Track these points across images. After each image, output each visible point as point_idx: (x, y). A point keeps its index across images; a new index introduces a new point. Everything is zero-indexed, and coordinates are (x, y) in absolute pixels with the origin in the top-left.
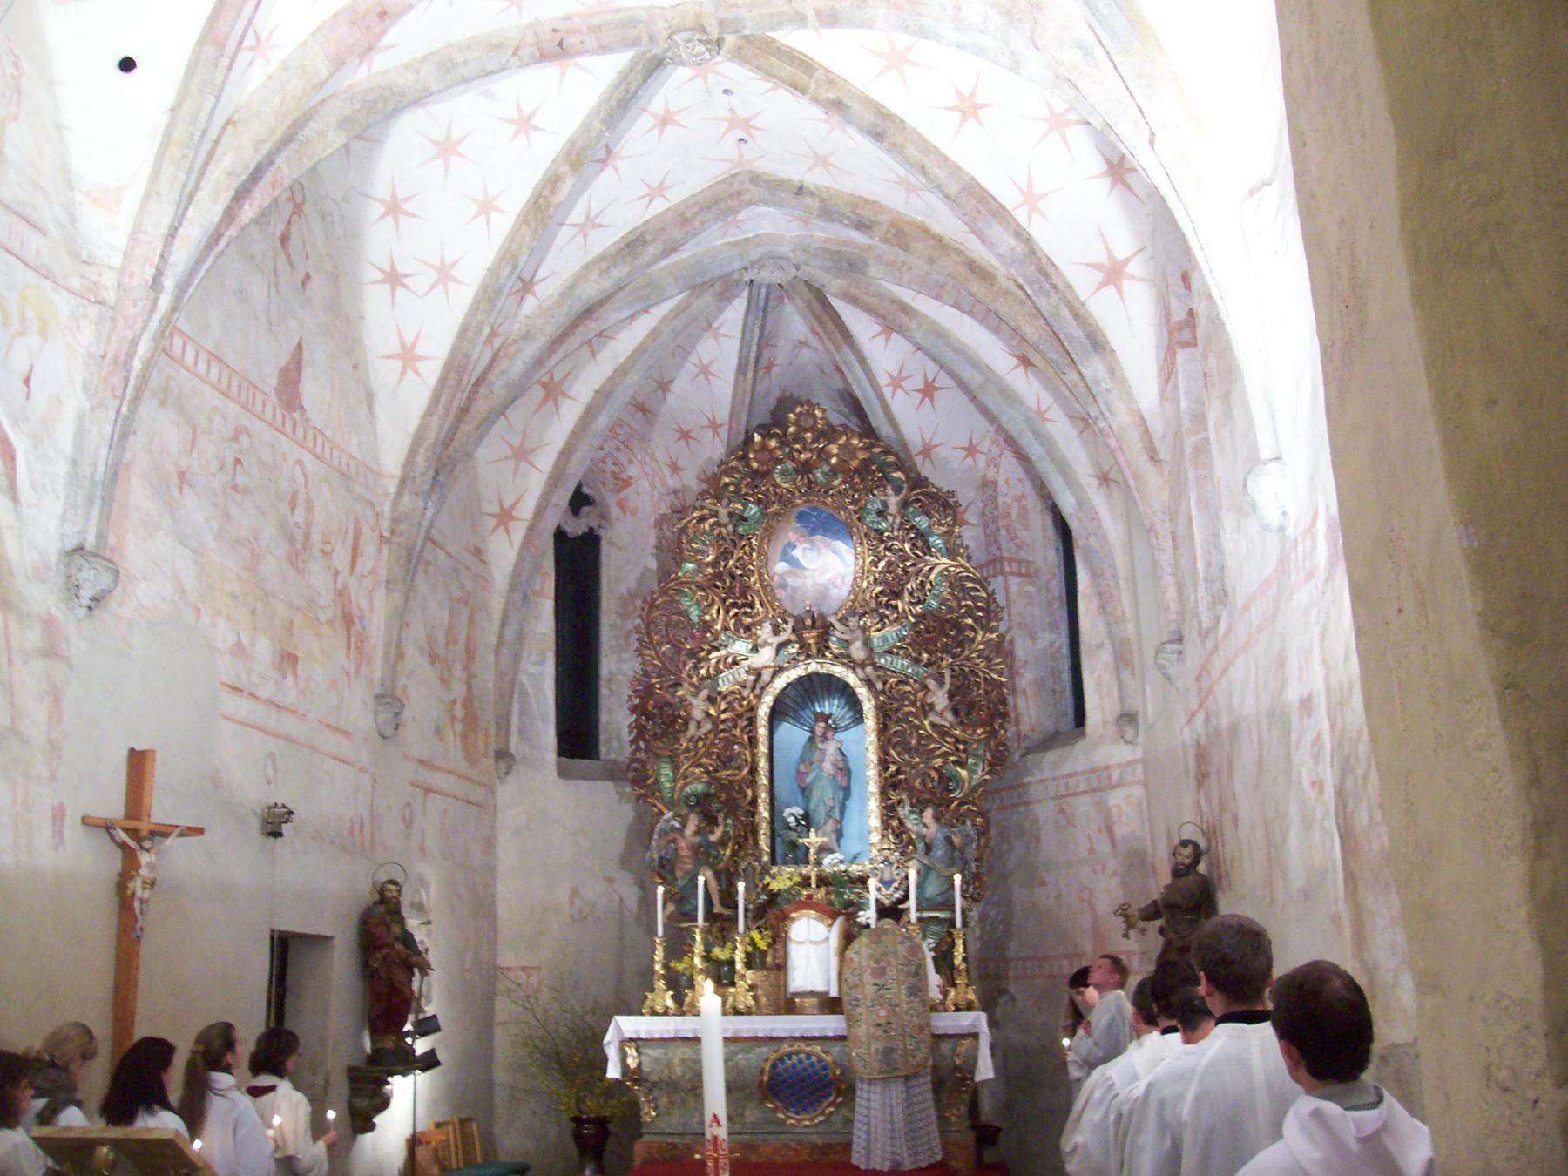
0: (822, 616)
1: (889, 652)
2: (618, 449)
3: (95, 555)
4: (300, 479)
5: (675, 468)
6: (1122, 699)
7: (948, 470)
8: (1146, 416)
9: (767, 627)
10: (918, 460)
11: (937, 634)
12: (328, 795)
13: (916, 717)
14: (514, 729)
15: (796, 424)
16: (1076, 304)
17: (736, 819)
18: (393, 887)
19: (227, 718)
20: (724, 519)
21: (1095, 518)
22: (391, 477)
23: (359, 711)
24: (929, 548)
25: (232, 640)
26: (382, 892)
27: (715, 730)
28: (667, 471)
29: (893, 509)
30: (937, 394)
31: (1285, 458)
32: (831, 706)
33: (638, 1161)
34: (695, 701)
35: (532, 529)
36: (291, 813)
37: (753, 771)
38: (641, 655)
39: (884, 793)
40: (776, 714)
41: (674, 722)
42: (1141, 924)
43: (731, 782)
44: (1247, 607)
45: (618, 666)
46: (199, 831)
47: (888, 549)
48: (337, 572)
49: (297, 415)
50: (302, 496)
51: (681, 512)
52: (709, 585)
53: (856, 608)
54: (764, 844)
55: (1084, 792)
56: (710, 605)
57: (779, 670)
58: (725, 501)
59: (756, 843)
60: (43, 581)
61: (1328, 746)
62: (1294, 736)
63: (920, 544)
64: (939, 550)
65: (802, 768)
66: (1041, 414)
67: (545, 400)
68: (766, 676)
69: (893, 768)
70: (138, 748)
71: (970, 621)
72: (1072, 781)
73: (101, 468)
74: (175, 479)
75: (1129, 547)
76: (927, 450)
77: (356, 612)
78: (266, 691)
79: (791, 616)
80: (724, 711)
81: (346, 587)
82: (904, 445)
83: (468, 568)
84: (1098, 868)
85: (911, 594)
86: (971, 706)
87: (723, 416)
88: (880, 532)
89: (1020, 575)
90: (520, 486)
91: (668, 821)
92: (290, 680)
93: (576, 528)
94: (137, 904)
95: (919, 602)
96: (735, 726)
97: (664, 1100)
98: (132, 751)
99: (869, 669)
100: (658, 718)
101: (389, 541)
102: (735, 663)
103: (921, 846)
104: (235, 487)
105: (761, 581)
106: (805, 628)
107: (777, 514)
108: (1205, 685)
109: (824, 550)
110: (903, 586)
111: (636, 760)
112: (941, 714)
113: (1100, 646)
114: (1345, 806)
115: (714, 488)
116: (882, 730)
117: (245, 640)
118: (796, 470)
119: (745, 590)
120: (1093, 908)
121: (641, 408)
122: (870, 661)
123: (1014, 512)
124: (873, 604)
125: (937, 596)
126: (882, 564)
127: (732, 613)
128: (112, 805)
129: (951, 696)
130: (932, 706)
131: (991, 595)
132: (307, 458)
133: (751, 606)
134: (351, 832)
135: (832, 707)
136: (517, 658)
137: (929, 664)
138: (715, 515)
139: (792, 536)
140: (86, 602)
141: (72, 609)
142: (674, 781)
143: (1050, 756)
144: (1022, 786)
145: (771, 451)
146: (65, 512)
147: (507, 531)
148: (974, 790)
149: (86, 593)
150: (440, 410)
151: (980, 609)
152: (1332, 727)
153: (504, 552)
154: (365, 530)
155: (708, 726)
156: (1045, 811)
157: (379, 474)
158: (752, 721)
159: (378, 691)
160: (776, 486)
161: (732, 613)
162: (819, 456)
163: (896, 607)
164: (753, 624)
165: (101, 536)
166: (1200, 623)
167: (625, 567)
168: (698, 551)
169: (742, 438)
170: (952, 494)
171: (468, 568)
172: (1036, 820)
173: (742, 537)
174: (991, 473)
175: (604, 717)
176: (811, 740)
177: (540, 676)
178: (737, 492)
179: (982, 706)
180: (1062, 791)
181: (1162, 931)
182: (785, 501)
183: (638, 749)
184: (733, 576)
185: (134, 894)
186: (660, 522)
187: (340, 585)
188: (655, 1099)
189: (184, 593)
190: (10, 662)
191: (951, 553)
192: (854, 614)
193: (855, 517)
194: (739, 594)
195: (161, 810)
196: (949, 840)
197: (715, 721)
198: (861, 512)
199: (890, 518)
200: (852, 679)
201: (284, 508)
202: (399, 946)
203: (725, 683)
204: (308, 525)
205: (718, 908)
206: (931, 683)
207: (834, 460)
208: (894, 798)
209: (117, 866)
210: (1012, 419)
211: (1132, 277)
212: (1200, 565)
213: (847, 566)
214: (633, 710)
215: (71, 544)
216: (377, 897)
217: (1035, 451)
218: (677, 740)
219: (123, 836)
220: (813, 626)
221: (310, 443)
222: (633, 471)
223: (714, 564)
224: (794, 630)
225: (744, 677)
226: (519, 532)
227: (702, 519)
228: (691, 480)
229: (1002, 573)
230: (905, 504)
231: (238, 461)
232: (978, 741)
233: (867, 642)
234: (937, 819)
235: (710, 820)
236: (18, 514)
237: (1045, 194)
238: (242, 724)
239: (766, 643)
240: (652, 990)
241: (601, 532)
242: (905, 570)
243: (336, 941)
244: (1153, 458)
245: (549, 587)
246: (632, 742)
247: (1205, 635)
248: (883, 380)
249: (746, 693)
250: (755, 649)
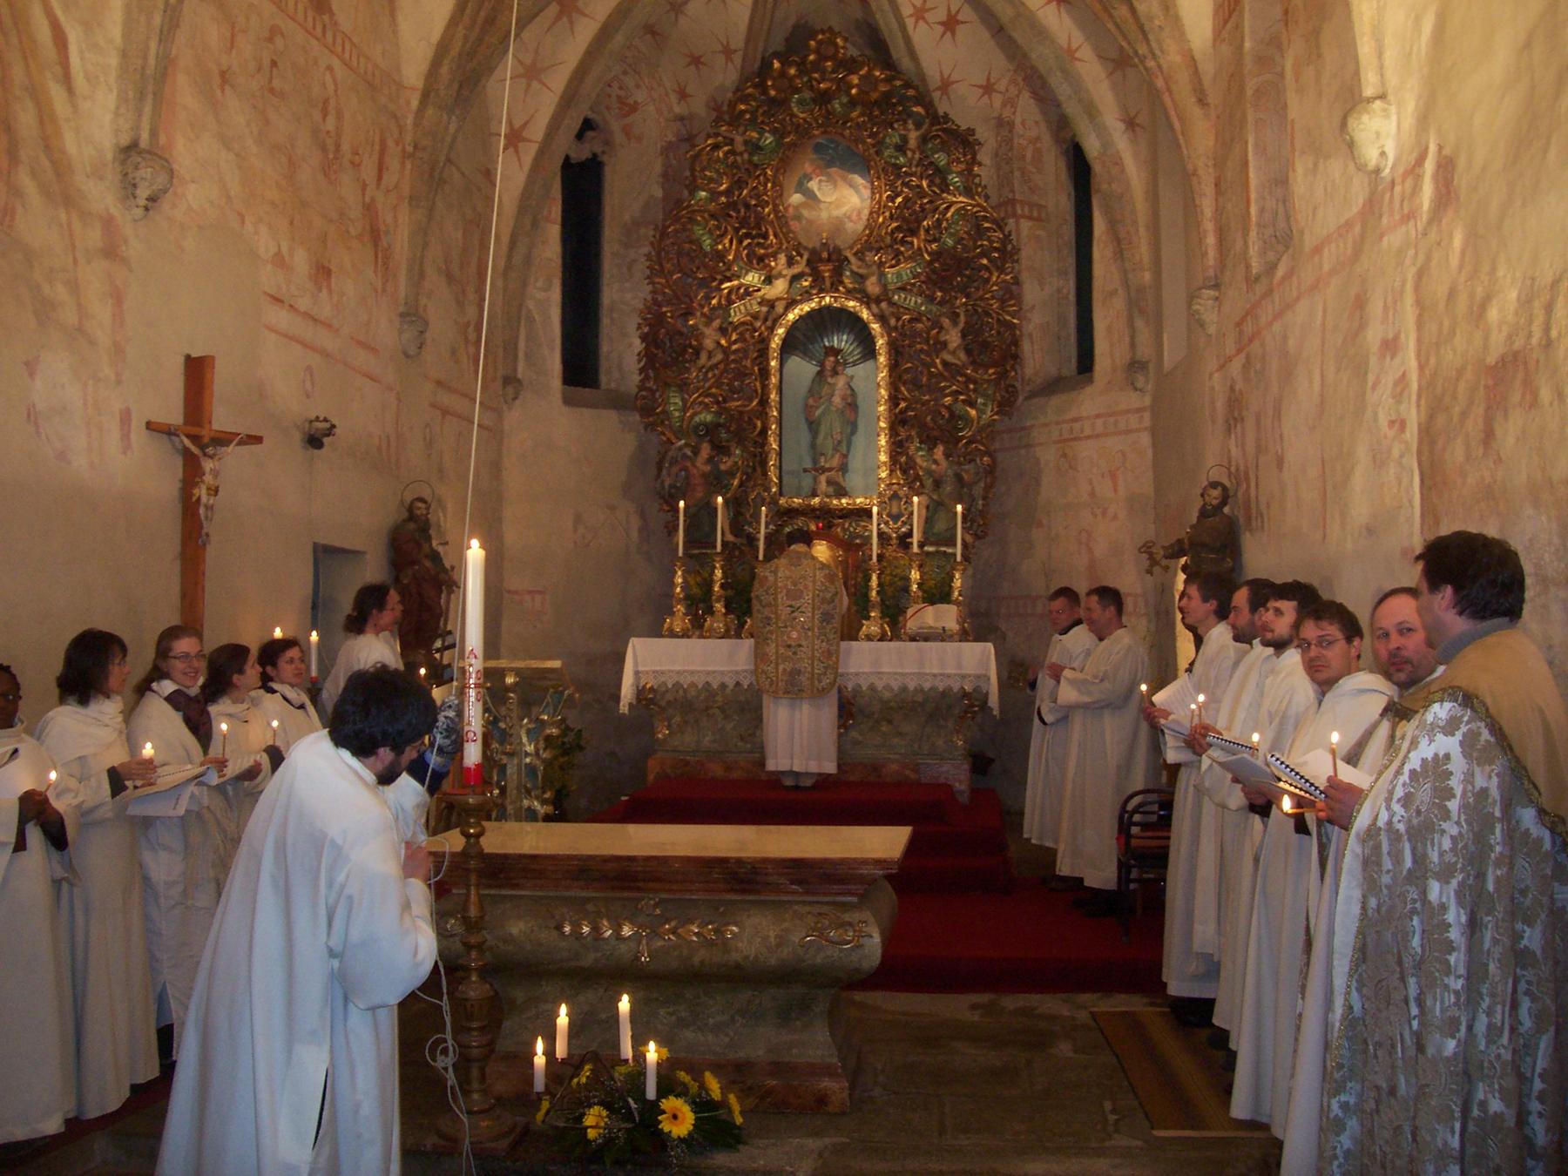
0: (838, 250)
1: (903, 289)
2: (625, 73)
3: (149, 152)
4: (331, 87)
5: (683, 95)
6: (1133, 345)
7: (966, 107)
8: (1197, 55)
9: (782, 258)
10: (936, 95)
11: (950, 273)
12: (360, 414)
13: (928, 354)
14: (521, 355)
15: (817, 52)
17: (744, 449)
18: (420, 504)
19: (267, 327)
20: (740, 147)
21: (1118, 162)
22: (413, 89)
23: (386, 330)
24: (947, 186)
25: (274, 250)
26: (410, 509)
27: (726, 360)
28: (673, 98)
29: (912, 143)
30: (960, 29)
31: (1391, 97)
32: (840, 341)
33: (651, 778)
34: (708, 331)
35: (541, 152)
36: (333, 426)
37: (764, 402)
38: (653, 283)
39: (893, 431)
40: (788, 347)
41: (684, 351)
42: (1164, 562)
43: (741, 413)
44: (1318, 250)
45: (624, 296)
46: (258, 440)
47: (905, 184)
48: (364, 187)
49: (326, 18)
50: (332, 102)
51: (690, 139)
52: (721, 215)
53: (871, 242)
54: (773, 475)
55: (1088, 437)
56: (723, 236)
57: (791, 304)
58: (741, 129)
59: (765, 474)
60: (101, 178)
61: (1415, 386)
62: (1371, 378)
63: (937, 181)
64: (957, 188)
65: (811, 401)
66: (1071, 53)
67: (558, 18)
68: (780, 308)
69: (903, 405)
70: (194, 355)
71: (985, 261)
72: (1077, 426)
73: (152, 62)
74: (217, 81)
75: (1153, 196)
76: (945, 86)
77: (382, 228)
78: (304, 303)
79: (806, 248)
80: (735, 342)
81: (373, 199)
82: (923, 79)
83: (479, 190)
84: (1099, 511)
85: (927, 231)
86: (985, 345)
87: (738, 42)
88: (898, 167)
89: (1030, 218)
90: (525, 106)
91: (680, 448)
92: (325, 291)
93: (581, 154)
94: (202, 511)
95: (935, 240)
96: (746, 357)
97: (677, 719)
98: (188, 358)
99: (884, 305)
100: (667, 350)
101: (411, 156)
102: (748, 293)
103: (929, 482)
104: (272, 91)
105: (775, 210)
106: (821, 260)
107: (793, 145)
108: (1249, 328)
109: (840, 183)
110: (919, 222)
111: (646, 389)
112: (953, 353)
113: (1113, 293)
114: (1433, 443)
115: (727, 114)
116: (893, 367)
117: (285, 250)
118: (814, 100)
119: (760, 219)
120: (1090, 550)
121: (651, 30)
122: (885, 296)
123: (1029, 156)
124: (888, 240)
125: (952, 235)
126: (900, 199)
127: (746, 243)
128: (173, 414)
129: (964, 336)
130: (945, 344)
131: (1007, 237)
132: (336, 63)
133: (765, 237)
134: (379, 449)
135: (841, 341)
136: (525, 284)
137: (942, 303)
138: (731, 142)
139: (808, 168)
140: (143, 202)
141: (128, 209)
142: (684, 409)
143: (1056, 401)
144: (1023, 428)
145: (791, 79)
146: (118, 108)
147: (517, 152)
148: (980, 430)
149: (143, 193)
150: (466, 18)
151: (996, 249)
152: (1421, 367)
153: (510, 175)
154: (390, 143)
155: (719, 357)
156: (1047, 456)
157: (400, 86)
158: (763, 353)
159: (402, 309)
160: (793, 115)
161: (746, 243)
162: (838, 87)
163: (912, 243)
164: (767, 256)
165: (154, 134)
166: (1248, 266)
167: (630, 193)
168: (711, 180)
169: (757, 65)
170: (972, 131)
171: (479, 190)
172: (1038, 462)
173: (756, 166)
174: (1006, 113)
175: (605, 348)
176: (820, 373)
177: (546, 301)
178: (753, 120)
179: (995, 349)
180: (1066, 436)
182: (803, 131)
183: (647, 378)
184: (747, 206)
185: (199, 499)
186: (668, 149)
187: (367, 199)
188: (669, 719)
189: (229, 198)
190: (75, 261)
191: (968, 192)
192: (870, 250)
193: (872, 151)
194: (756, 226)
195: (221, 418)
196: (959, 477)
197: (726, 351)
198: (879, 146)
199: (909, 154)
200: (865, 314)
201: (317, 116)
202: (428, 564)
203: (738, 313)
204: (339, 135)
205: (730, 538)
206: (946, 322)
207: (854, 91)
208: (903, 434)
209: (180, 475)
210: (1040, 55)
212: (1253, 210)
213: (863, 201)
214: (644, 338)
215: (125, 140)
216: (405, 515)
217: (1062, 90)
218: (688, 370)
219: (187, 442)
220: (829, 260)
221: (339, 49)
222: (640, 96)
223: (728, 193)
224: (809, 263)
225: (756, 308)
226: (529, 152)
227: (716, 147)
228: (698, 106)
229: (1014, 215)
230: (924, 140)
231: (274, 64)
232: (988, 381)
233: (882, 275)
234: (947, 455)
235: (720, 449)
236: (74, 106)
238: (286, 336)
239: (780, 275)
240: (672, 614)
241: (604, 158)
242: (923, 209)
243: (368, 556)
244: (1202, 101)
245: (556, 211)
246: (641, 371)
247: (1252, 281)
248: (907, 11)
249: (758, 324)
250: (769, 280)
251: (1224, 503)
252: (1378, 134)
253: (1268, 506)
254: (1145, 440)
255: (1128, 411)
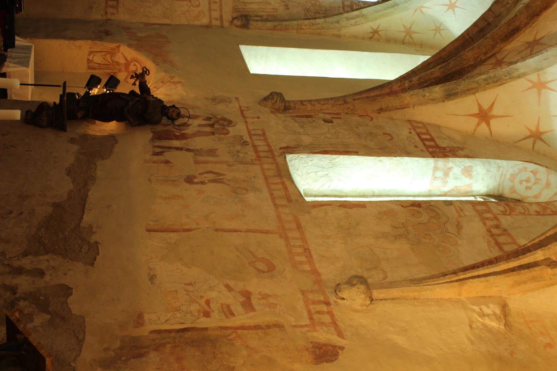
8: (404, 110)
16: (474, 91)
42: (137, 83)
181: (132, 92)
211: (478, 124)
237: (540, 95)
251: (169, 118)
252: (354, 300)
253: (167, 162)
254: (205, 21)
255: (221, 10)
